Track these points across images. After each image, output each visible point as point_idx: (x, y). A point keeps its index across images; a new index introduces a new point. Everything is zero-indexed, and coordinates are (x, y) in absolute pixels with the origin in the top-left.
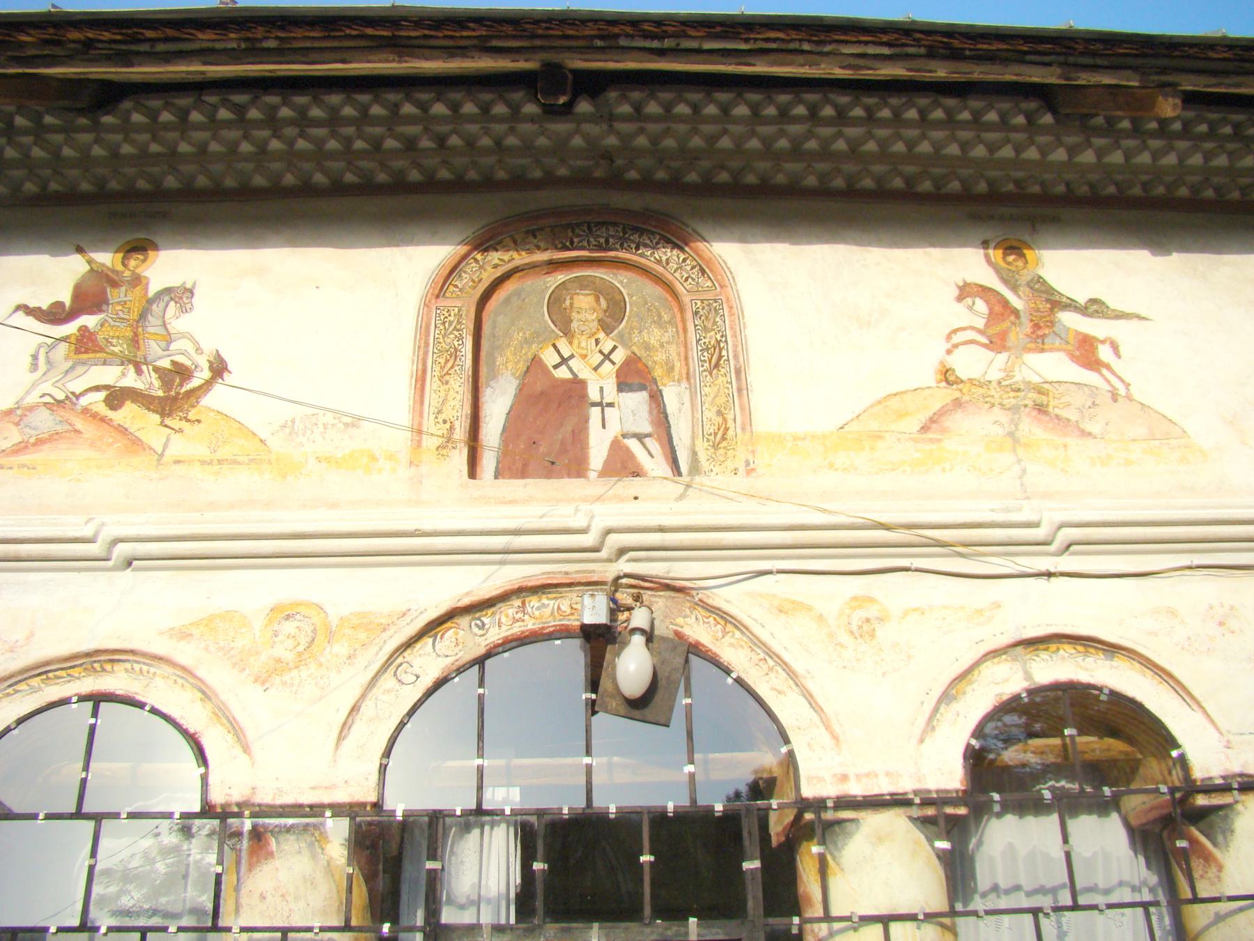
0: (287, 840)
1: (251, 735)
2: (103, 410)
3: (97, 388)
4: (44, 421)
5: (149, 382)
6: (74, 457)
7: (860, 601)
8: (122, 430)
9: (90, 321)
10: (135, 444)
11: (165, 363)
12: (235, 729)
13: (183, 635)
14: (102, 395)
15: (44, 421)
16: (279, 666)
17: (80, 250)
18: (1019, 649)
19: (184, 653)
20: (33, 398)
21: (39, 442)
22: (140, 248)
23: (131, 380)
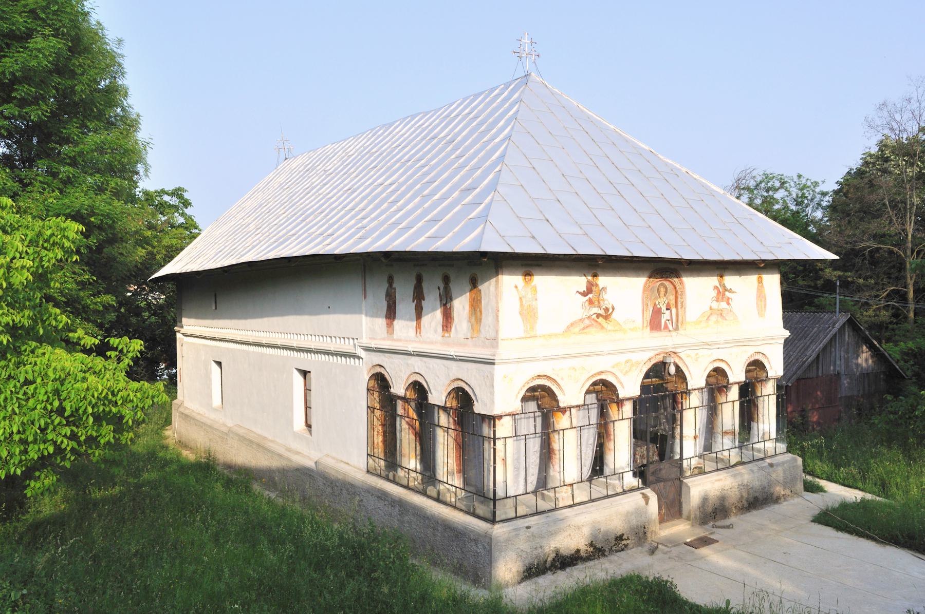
0: (183, 444)
1: (624, 385)
2: (596, 318)
3: (594, 314)
4: (587, 322)
5: (602, 312)
6: (592, 330)
7: (697, 354)
8: (600, 324)
9: (590, 296)
10: (603, 327)
11: (604, 307)
12: (621, 384)
13: (613, 367)
14: (595, 315)
15: (587, 322)
16: (627, 372)
17: (585, 275)
18: (718, 361)
19: (613, 371)
20: (584, 317)
21: (587, 327)
22: (595, 275)
23: (600, 312)
